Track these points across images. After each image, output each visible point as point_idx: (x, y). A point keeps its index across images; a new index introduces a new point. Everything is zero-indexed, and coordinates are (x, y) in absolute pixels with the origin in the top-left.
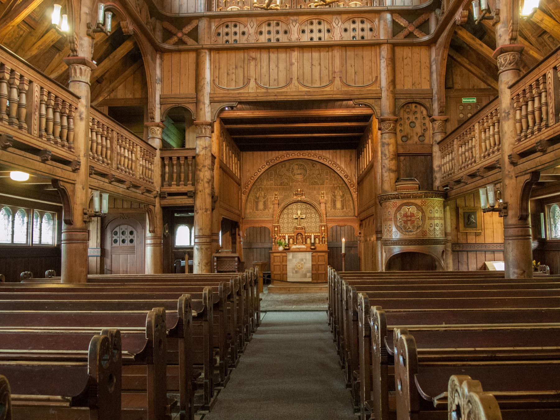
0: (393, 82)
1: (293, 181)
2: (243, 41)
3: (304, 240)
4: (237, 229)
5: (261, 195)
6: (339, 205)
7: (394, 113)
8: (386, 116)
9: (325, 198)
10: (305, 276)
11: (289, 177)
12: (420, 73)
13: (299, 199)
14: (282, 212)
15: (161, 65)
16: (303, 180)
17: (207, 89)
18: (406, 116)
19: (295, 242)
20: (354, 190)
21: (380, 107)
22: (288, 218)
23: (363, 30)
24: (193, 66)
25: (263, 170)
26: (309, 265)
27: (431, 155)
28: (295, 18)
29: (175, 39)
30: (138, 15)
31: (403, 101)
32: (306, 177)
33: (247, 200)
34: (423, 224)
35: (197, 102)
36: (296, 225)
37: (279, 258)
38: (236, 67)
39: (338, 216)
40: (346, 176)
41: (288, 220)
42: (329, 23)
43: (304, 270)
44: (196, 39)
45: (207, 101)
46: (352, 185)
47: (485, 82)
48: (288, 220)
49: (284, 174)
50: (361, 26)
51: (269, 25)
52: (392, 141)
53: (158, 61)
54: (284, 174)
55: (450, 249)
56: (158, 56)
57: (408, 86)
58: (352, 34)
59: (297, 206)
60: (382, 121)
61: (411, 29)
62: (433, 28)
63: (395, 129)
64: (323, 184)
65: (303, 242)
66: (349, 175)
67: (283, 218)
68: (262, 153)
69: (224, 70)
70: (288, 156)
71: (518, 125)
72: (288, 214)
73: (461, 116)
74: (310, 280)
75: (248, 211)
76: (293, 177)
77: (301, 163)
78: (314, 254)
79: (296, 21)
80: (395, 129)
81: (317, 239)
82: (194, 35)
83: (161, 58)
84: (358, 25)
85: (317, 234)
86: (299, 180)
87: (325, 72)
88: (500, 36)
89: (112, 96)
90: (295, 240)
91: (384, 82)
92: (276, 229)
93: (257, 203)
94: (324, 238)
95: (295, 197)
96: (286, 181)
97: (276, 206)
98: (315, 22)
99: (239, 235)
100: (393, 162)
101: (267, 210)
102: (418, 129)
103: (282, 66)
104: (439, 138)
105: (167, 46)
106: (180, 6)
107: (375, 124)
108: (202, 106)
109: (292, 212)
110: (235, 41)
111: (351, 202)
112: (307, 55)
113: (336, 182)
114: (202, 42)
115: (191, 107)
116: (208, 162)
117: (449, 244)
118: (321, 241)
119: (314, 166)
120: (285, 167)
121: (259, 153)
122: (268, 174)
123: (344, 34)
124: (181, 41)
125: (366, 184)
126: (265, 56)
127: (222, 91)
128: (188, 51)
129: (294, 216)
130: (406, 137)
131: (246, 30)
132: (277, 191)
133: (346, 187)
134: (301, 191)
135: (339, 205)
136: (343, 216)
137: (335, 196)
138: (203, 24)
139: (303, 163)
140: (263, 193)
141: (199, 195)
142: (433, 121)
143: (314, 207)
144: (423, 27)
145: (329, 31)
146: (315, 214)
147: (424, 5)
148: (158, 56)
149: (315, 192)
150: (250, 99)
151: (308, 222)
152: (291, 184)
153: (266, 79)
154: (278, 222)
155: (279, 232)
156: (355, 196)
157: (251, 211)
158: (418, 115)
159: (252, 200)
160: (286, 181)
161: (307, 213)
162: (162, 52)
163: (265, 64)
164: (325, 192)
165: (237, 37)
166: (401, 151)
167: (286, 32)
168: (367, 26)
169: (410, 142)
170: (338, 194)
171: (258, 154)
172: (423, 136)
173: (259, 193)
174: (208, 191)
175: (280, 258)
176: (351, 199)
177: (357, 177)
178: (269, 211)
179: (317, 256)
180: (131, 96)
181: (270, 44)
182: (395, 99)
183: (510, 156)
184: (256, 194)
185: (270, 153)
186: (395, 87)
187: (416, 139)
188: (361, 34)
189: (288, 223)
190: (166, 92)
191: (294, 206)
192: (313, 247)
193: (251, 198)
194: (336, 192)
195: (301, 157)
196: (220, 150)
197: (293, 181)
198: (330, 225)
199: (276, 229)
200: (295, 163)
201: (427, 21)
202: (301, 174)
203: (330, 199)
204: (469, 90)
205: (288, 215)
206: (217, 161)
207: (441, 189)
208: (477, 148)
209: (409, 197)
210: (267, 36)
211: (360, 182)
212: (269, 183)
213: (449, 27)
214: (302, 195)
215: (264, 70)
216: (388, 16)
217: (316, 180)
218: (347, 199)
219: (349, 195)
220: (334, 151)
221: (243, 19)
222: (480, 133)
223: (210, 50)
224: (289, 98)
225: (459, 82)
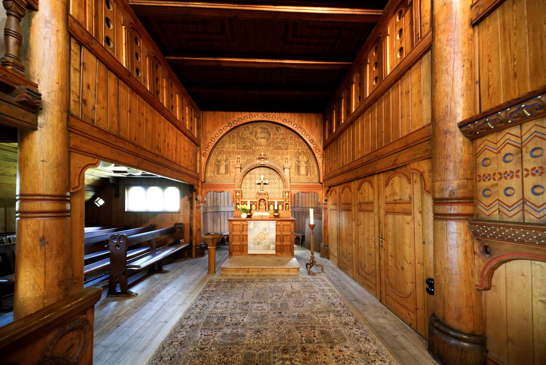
1: (256, 145)
3: (267, 206)
4: (194, 193)
5: (222, 158)
6: (303, 171)
9: (290, 164)
10: (268, 248)
11: (252, 140)
13: (262, 163)
16: (266, 144)
19: (258, 209)
20: (320, 156)
22: (251, 183)
25: (224, 132)
32: (269, 141)
37: (238, 226)
43: (267, 242)
46: (317, 151)
49: (247, 138)
54: (247, 138)
65: (266, 209)
66: (315, 139)
67: (246, 183)
68: (224, 113)
70: (251, 117)
72: (251, 179)
74: (274, 252)
75: (209, 175)
77: (265, 126)
78: (279, 223)
81: (280, 206)
85: (280, 201)
90: (258, 206)
92: (238, 194)
93: (218, 167)
94: (288, 204)
95: (258, 161)
96: (249, 144)
97: (239, 170)
99: (197, 199)
101: (229, 174)
109: (255, 177)
111: (316, 168)
113: (300, 147)
118: (284, 207)
119: (278, 130)
120: (248, 130)
121: (221, 113)
122: (230, 137)
132: (239, 154)
133: (311, 153)
137: (299, 162)
139: (267, 127)
140: (224, 156)
146: (279, 180)
149: (279, 157)
152: (254, 148)
155: (240, 198)
156: (320, 161)
157: (212, 175)
159: (214, 165)
160: (249, 144)
161: (271, 179)
164: (289, 157)
171: (220, 114)
173: (220, 156)
175: (240, 227)
176: (315, 165)
177: (322, 142)
178: (230, 175)
179: (282, 225)
184: (218, 157)
185: (231, 113)
189: (250, 188)
191: (257, 171)
192: (276, 214)
193: (212, 160)
194: (300, 157)
195: (265, 119)
197: (256, 145)
198: (294, 191)
199: (238, 194)
200: (259, 127)
202: (264, 138)
203: (294, 165)
205: (251, 180)
212: (231, 146)
214: (266, 159)
217: (280, 145)
218: (311, 165)
219: (314, 161)
220: (300, 114)
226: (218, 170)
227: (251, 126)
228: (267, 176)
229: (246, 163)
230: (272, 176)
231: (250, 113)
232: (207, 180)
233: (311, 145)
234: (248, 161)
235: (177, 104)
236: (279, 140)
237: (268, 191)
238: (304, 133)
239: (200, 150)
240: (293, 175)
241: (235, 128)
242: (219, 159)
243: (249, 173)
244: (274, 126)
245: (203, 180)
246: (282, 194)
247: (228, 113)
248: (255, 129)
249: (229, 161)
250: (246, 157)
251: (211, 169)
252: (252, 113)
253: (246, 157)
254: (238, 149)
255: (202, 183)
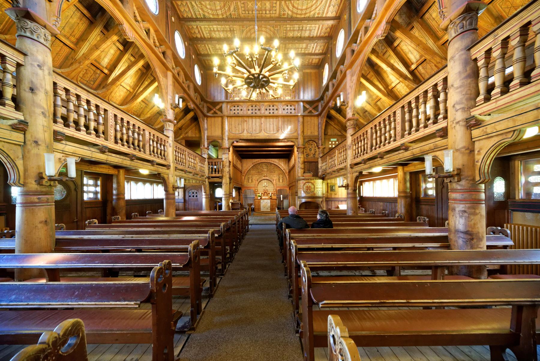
0: (303, 132)
1: (263, 171)
2: (241, 113)
6: (281, 181)
7: (303, 145)
8: (300, 146)
10: (268, 209)
12: (314, 128)
14: (258, 183)
15: (207, 123)
17: (226, 134)
18: (308, 146)
19: (264, 195)
21: (298, 142)
23: (291, 109)
24: (220, 124)
26: (269, 205)
27: (318, 162)
28: (263, 103)
29: (212, 112)
30: (195, 101)
31: (307, 140)
34: (314, 190)
35: (222, 139)
38: (239, 124)
40: (284, 169)
42: (277, 106)
43: (267, 207)
44: (221, 112)
45: (227, 139)
47: (340, 132)
50: (290, 108)
51: (252, 106)
52: (302, 156)
53: (205, 121)
55: (324, 200)
56: (205, 119)
57: (309, 134)
58: (287, 111)
60: (298, 148)
61: (311, 109)
62: (320, 109)
63: (303, 151)
69: (233, 126)
71: (354, 152)
73: (330, 146)
75: (245, 183)
79: (263, 105)
80: (303, 151)
82: (221, 110)
83: (207, 120)
84: (289, 107)
87: (275, 127)
88: (348, 113)
89: (186, 135)
91: (300, 132)
98: (271, 106)
100: (303, 165)
102: (313, 152)
103: (258, 124)
104: (321, 155)
105: (209, 114)
106: (214, 97)
107: (296, 149)
108: (224, 141)
110: (238, 113)
112: (268, 120)
114: (224, 113)
115: (220, 141)
116: (228, 164)
117: (324, 198)
123: (283, 111)
124: (215, 113)
125: (292, 172)
126: (250, 120)
127: (232, 135)
128: (218, 117)
130: (308, 155)
131: (242, 108)
138: (224, 106)
141: (224, 178)
142: (319, 148)
143: (271, 182)
144: (316, 108)
145: (277, 110)
147: (317, 99)
148: (205, 119)
150: (245, 138)
153: (251, 130)
156: (287, 177)
158: (313, 146)
162: (208, 117)
163: (250, 123)
165: (239, 111)
166: (306, 160)
167: (259, 110)
168: (293, 108)
169: (309, 157)
172: (315, 154)
174: (228, 176)
180: (194, 136)
181: (252, 115)
182: (304, 139)
183: (350, 165)
186: (304, 134)
187: (312, 155)
188: (290, 111)
190: (209, 134)
191: (263, 181)
196: (233, 159)
197: (263, 171)
198: (278, 189)
201: (317, 106)
204: (334, 135)
206: (231, 163)
207: (321, 176)
208: (337, 160)
209: (308, 180)
210: (251, 111)
211: (289, 172)
213: (326, 109)
215: (250, 126)
216: (302, 104)
221: (241, 104)
222: (338, 154)
223: (228, 117)
224: (261, 138)
225: (330, 132)
226: (249, 181)
227: (261, 164)
229: (259, 178)
234: (260, 177)
240: (277, 183)
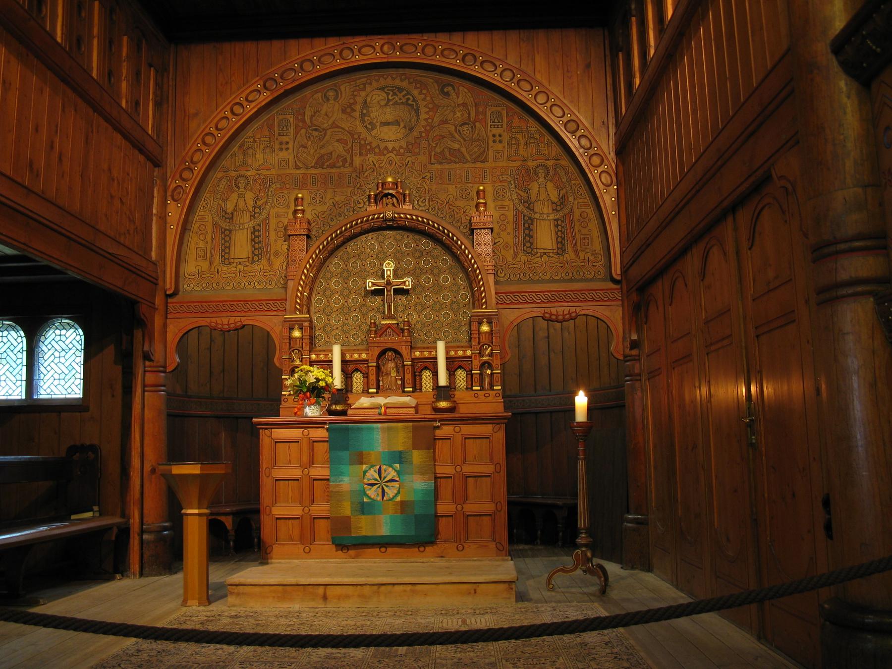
3: (409, 376)
4: (138, 334)
5: (241, 205)
6: (545, 238)
11: (352, 134)
13: (389, 214)
14: (320, 266)
16: (404, 145)
25: (251, 109)
32: (415, 133)
33: (185, 227)
36: (379, 317)
39: (543, 281)
41: (346, 298)
46: (596, 160)
48: (346, 298)
49: (334, 125)
54: (334, 125)
59: (381, 244)
64: (481, 158)
65: (403, 386)
68: (250, 47)
70: (346, 53)
72: (345, 275)
75: (191, 266)
76: (365, 134)
77: (398, 82)
81: (461, 375)
85: (460, 353)
86: (390, 146)
90: (373, 377)
92: (297, 334)
93: (226, 235)
94: (490, 366)
95: (373, 208)
96: (339, 148)
97: (300, 243)
99: (147, 357)
111: (594, 225)
118: (476, 378)
119: (447, 94)
120: (336, 98)
122: (271, 127)
129: (369, 285)
132: (303, 186)
133: (572, 168)
134: (396, 184)
135: (545, 238)
136: (564, 281)
137: (529, 204)
139: (405, 84)
140: (249, 196)
143: (448, 248)
149: (452, 189)
151: (424, 307)
152: (357, 161)
154: (307, 305)
155: (306, 347)
156: (608, 198)
157: (205, 265)
159: (209, 229)
160: (339, 148)
161: (423, 271)
164: (489, 189)
170: (543, 196)
173: (234, 196)
175: (301, 449)
176: (591, 213)
177: (612, 131)
178: (271, 264)
179: (458, 440)
184: (225, 201)
185: (277, 44)
189: (346, 310)
191: (370, 243)
192: (443, 404)
193: (205, 214)
194: (534, 187)
195: (398, 56)
197: (366, 148)
199: (297, 334)
200: (374, 84)
202: (397, 123)
203: (510, 215)
214: (403, 198)
217: (456, 146)
218: (577, 213)
226: (226, 248)
227: (346, 87)
228: (408, 263)
230: (427, 262)
231: (345, 39)
232: (184, 286)
233: (572, 142)
235: (95, 31)
236: (452, 128)
237: (415, 318)
238: (541, 99)
239: (164, 180)
241: (287, 93)
242: (230, 207)
243: (340, 253)
244: (430, 78)
245: (169, 285)
246: (465, 328)
247: (263, 45)
248: (363, 94)
249: (264, 214)
250: (329, 195)
251: (201, 244)
252: (349, 40)
253: (329, 195)
254: (297, 167)
255: (170, 296)
